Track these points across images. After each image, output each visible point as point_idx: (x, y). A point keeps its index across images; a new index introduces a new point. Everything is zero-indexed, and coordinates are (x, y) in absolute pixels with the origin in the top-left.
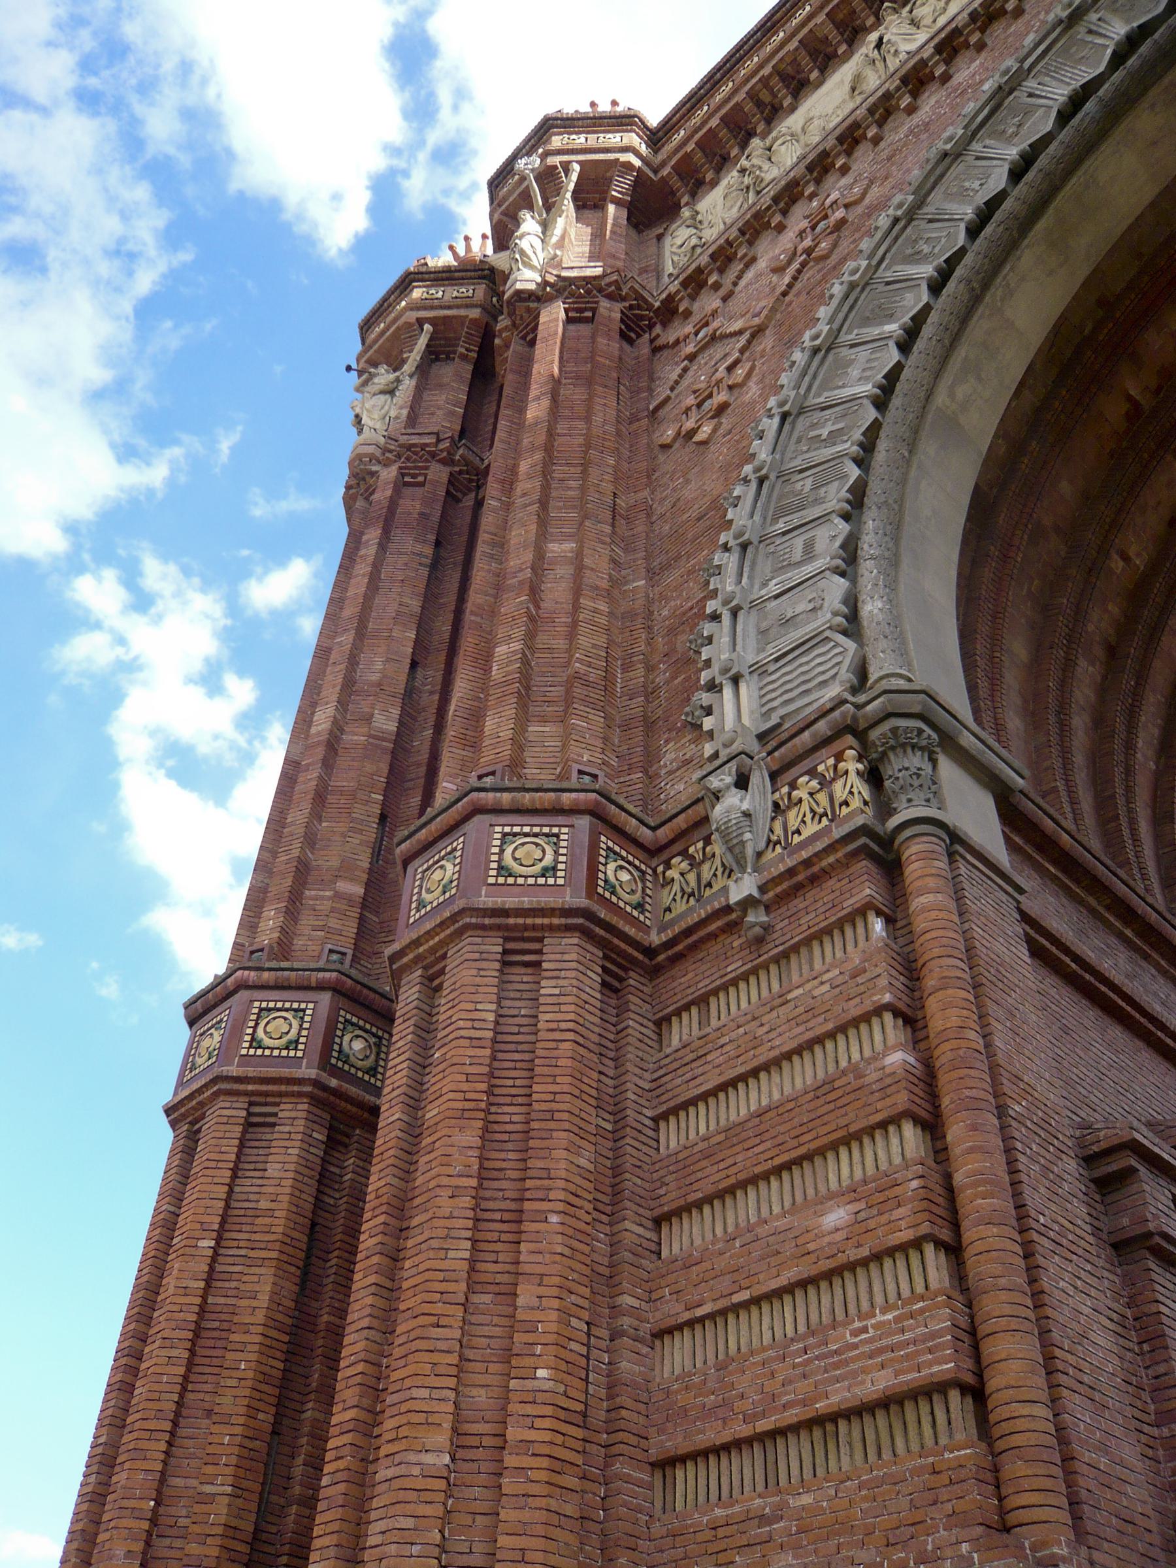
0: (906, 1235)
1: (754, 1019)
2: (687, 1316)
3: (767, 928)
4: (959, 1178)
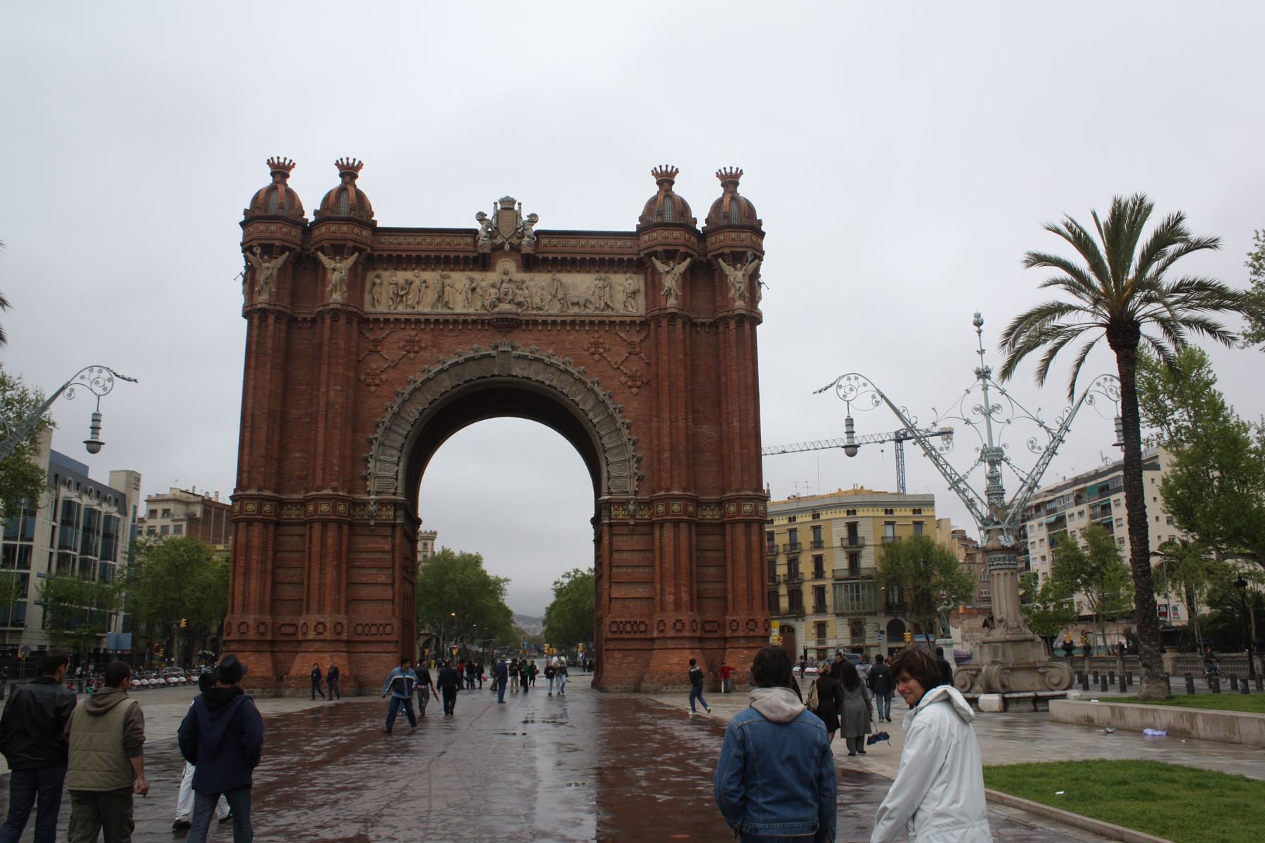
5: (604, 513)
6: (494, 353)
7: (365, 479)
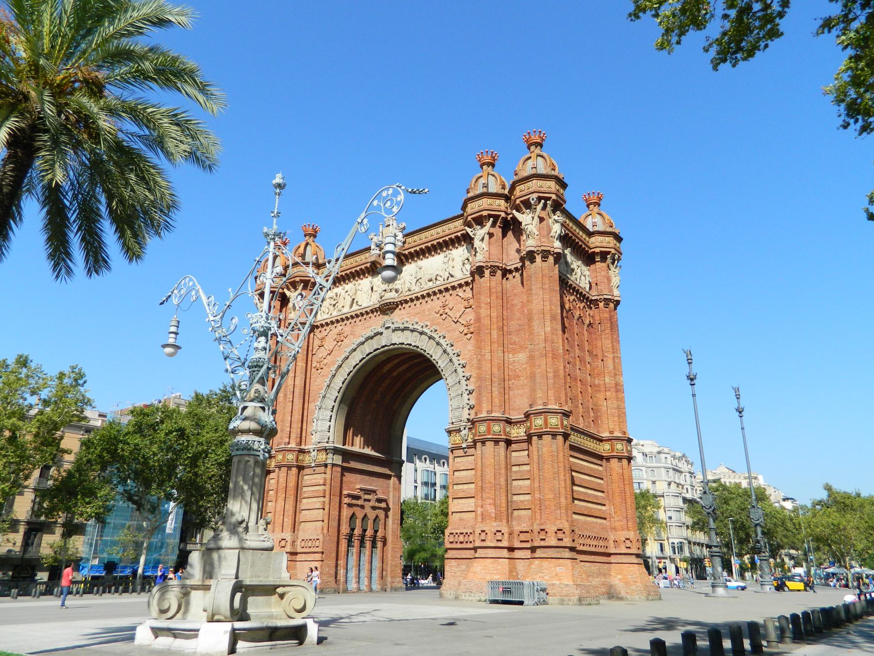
6: (381, 330)
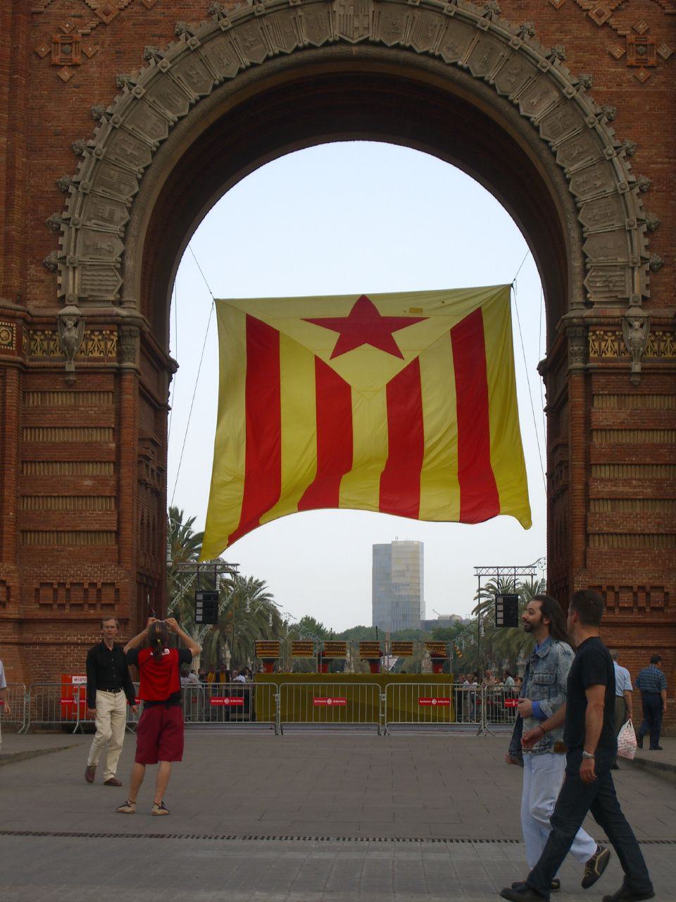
0: (107, 494)
1: (66, 410)
2: (35, 494)
3: (75, 381)
4: (123, 482)
5: (575, 347)
7: (54, 271)
